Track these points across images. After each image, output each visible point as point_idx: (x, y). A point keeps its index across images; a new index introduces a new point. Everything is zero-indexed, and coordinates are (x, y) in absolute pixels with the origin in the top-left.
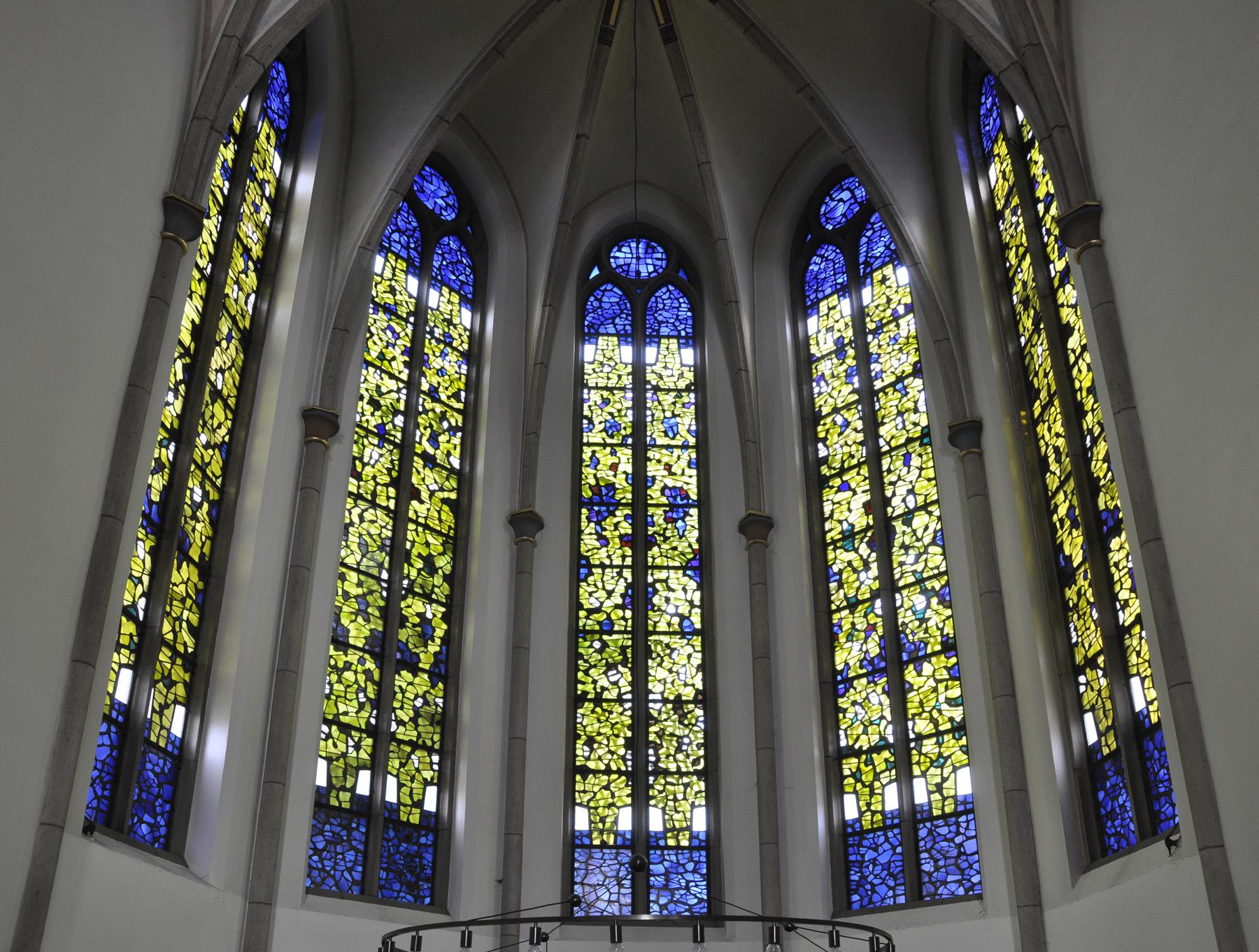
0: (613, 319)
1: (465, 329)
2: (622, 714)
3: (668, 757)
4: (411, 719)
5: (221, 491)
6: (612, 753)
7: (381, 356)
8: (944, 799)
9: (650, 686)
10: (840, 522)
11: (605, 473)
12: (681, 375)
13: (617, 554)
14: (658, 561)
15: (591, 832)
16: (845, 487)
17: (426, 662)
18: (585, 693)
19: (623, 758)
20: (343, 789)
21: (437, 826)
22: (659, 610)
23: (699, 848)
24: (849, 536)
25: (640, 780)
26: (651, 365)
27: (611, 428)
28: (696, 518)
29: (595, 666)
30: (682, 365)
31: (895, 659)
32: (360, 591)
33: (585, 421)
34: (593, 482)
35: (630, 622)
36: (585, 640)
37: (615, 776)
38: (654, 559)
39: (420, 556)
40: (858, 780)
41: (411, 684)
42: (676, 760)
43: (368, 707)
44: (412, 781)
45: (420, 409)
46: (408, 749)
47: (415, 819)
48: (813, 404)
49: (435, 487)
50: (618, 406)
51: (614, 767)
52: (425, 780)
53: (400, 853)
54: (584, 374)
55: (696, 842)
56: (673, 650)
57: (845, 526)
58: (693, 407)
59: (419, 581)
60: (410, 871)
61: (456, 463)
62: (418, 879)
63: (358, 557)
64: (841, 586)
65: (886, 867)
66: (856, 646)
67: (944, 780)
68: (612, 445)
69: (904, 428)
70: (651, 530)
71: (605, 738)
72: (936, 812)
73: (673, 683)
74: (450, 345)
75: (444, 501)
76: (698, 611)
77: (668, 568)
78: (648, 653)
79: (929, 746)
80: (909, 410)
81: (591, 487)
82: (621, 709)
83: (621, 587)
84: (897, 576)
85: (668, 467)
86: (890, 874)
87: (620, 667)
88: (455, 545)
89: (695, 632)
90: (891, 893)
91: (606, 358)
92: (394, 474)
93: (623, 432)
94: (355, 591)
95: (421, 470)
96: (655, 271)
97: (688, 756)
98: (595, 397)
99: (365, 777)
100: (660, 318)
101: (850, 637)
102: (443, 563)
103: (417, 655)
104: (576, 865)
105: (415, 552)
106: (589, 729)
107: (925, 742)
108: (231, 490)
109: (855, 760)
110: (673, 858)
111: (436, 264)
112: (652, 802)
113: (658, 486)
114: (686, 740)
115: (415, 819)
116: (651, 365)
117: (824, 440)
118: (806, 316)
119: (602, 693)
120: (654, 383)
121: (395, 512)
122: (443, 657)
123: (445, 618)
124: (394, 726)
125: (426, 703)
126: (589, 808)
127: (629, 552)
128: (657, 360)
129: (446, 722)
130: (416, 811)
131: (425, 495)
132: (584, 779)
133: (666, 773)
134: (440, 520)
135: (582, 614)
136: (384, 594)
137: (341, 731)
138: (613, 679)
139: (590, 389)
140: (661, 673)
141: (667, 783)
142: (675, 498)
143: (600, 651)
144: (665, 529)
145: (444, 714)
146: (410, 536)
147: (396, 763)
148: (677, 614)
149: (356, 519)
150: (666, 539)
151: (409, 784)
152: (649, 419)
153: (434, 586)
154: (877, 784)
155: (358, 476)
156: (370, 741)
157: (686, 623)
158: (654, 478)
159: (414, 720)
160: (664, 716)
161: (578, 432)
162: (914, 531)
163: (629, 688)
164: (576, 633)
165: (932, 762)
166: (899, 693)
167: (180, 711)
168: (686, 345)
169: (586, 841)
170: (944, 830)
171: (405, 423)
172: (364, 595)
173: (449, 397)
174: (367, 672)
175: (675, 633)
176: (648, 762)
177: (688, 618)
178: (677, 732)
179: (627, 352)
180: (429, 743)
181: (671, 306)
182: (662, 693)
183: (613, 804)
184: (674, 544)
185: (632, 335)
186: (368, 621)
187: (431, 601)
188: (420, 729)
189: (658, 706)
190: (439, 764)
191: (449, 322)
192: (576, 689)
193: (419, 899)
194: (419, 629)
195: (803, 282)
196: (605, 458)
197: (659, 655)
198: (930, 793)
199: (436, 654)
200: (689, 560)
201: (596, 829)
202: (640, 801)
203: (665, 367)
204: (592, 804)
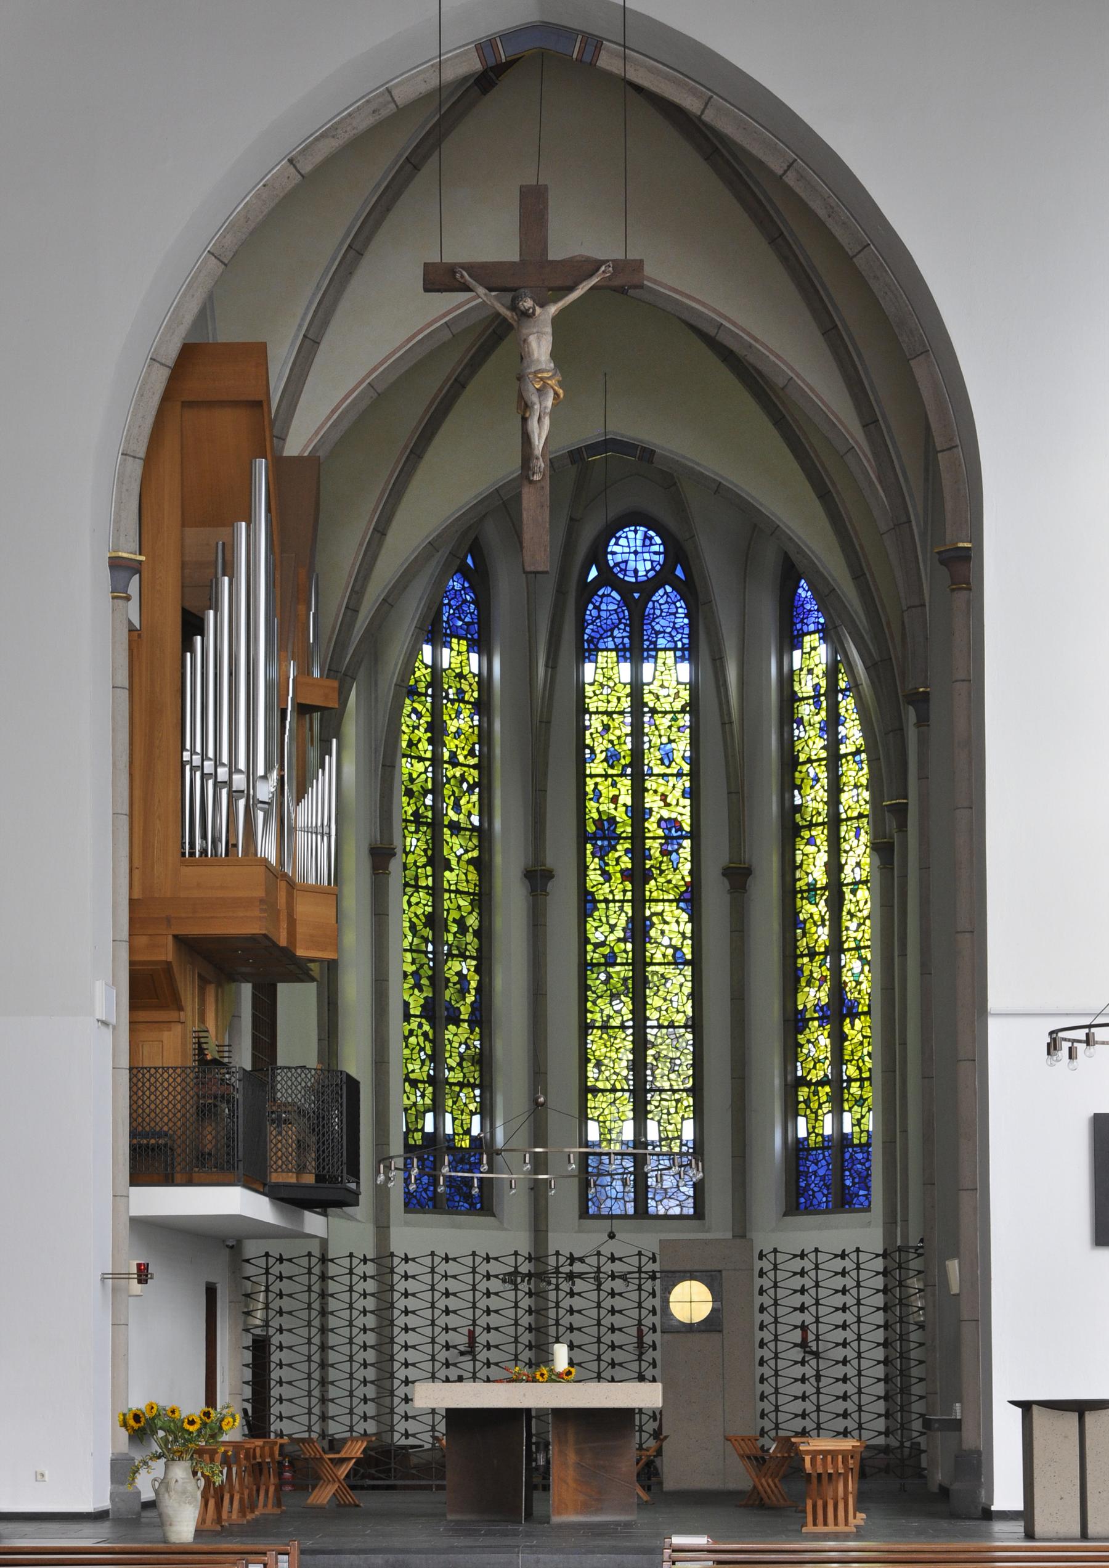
0: (612, 630)
9: (648, 1013)
10: (807, 874)
11: (606, 806)
12: (677, 695)
13: (619, 889)
14: (655, 895)
19: (626, 1079)
22: (656, 942)
25: (640, 1096)
28: (688, 850)
29: (601, 997)
30: (679, 683)
33: (587, 751)
34: (596, 816)
35: (630, 954)
38: (651, 892)
39: (454, 921)
40: (808, 1107)
41: (455, 1035)
42: (669, 1079)
46: (457, 1089)
47: (466, 1144)
50: (618, 733)
51: (618, 1087)
56: (667, 980)
58: (688, 731)
64: (804, 935)
65: (823, 1178)
68: (612, 776)
73: (666, 1010)
76: (689, 942)
77: (663, 901)
78: (645, 982)
81: (594, 821)
82: (623, 1035)
85: (664, 797)
86: (825, 1185)
88: (480, 900)
89: (686, 963)
90: (824, 1199)
93: (623, 762)
95: (449, 840)
96: (653, 568)
97: (679, 1075)
100: (657, 628)
101: (809, 984)
103: (458, 1009)
106: (597, 1053)
109: (807, 1089)
112: (650, 1116)
113: (655, 818)
115: (466, 1144)
119: (608, 1021)
120: (651, 705)
125: (468, 1048)
127: (629, 886)
128: (654, 678)
129: (483, 1060)
132: (595, 1097)
133: (661, 1091)
135: (590, 948)
138: (616, 1008)
139: (591, 714)
141: (662, 1099)
142: (670, 830)
143: (606, 982)
144: (661, 862)
145: (481, 1054)
147: (450, 1102)
148: (671, 946)
152: (646, 746)
154: (820, 1112)
157: (678, 955)
158: (651, 809)
159: (460, 1064)
160: (659, 1041)
161: (581, 762)
163: (630, 1016)
168: (683, 659)
176: (646, 1081)
177: (680, 949)
178: (671, 1055)
180: (472, 1081)
182: (658, 1020)
184: (669, 877)
185: (630, 650)
187: (465, 958)
188: (465, 1070)
189: (655, 1031)
192: (586, 1018)
194: (458, 986)
196: (607, 791)
199: (472, 1004)
200: (682, 893)
202: (640, 1115)
203: (662, 686)
204: (601, 1119)
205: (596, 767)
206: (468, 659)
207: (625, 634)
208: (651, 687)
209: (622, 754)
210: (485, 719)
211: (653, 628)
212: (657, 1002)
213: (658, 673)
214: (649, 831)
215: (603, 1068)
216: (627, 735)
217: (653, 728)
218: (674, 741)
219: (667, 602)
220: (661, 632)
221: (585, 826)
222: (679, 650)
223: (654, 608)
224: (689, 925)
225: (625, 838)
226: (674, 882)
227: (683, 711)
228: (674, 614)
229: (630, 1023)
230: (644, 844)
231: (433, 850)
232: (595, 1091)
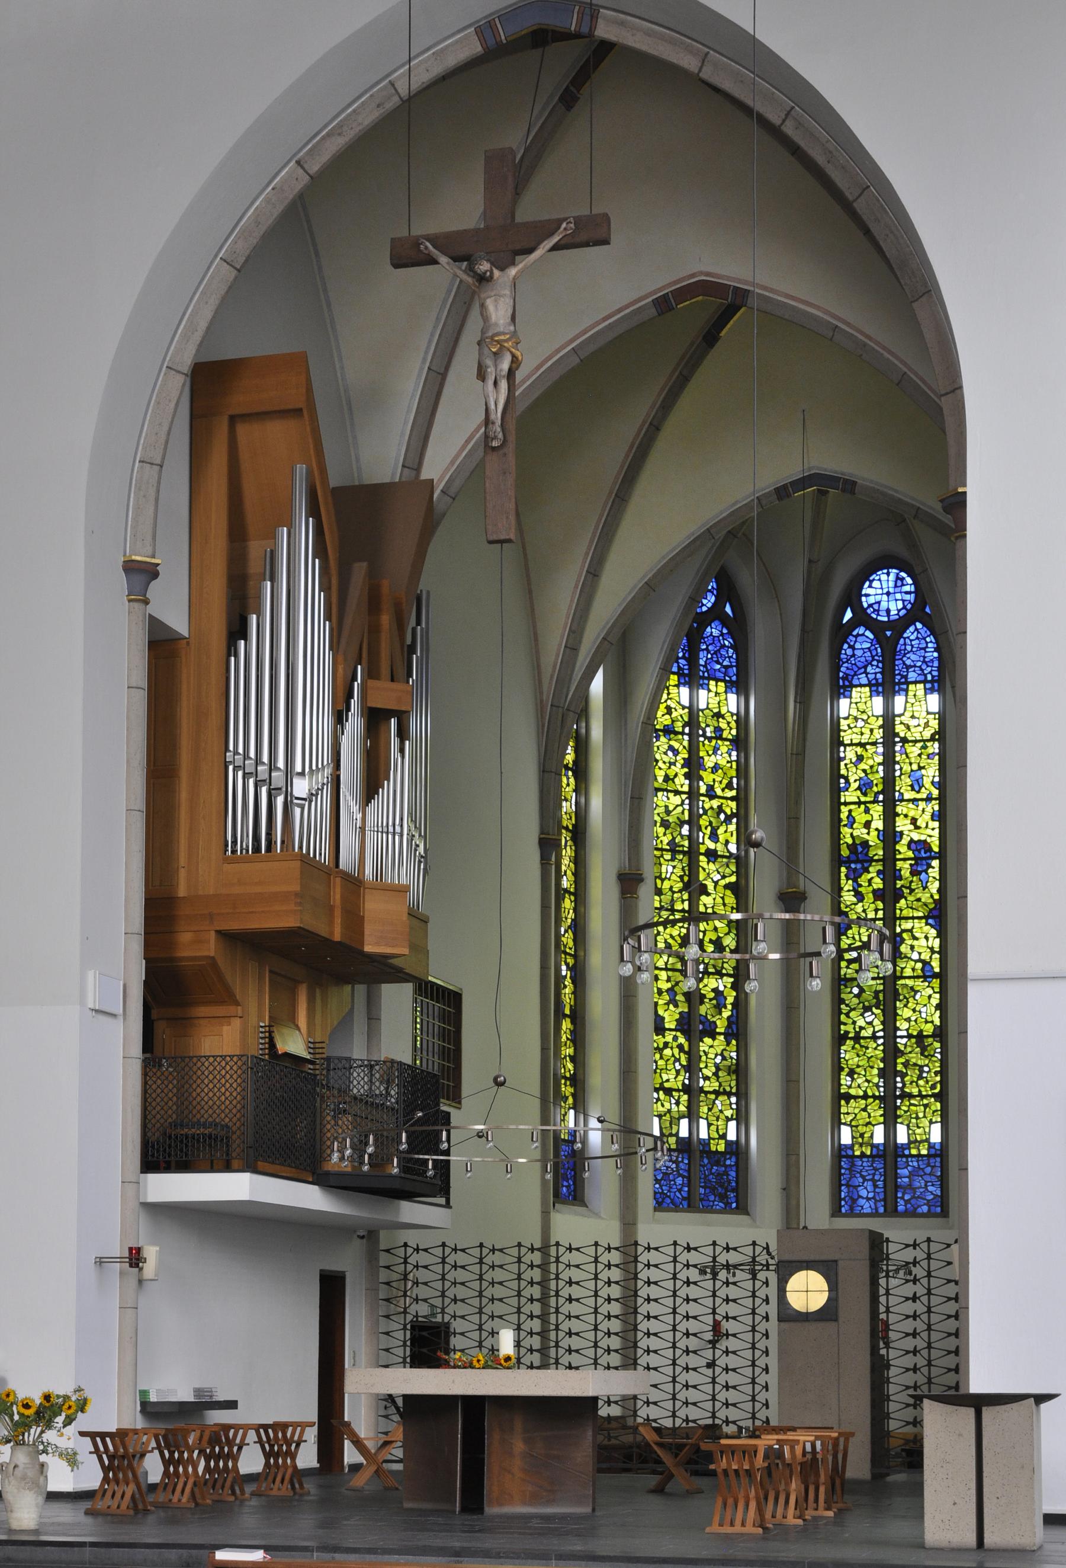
0: (865, 667)
1: (732, 715)
2: (876, 1049)
3: (911, 1083)
4: (714, 1074)
6: (868, 1081)
7: (667, 779)
11: (860, 832)
12: (927, 725)
13: (871, 909)
14: (905, 913)
15: (853, 1145)
17: (721, 1026)
18: (847, 1032)
19: (877, 1086)
20: (671, 1135)
21: (737, 1150)
22: (906, 957)
23: (935, 1156)
26: (899, 716)
27: (865, 786)
28: (937, 869)
29: (854, 1009)
30: (928, 713)
32: (669, 985)
33: (842, 781)
34: (850, 841)
36: (846, 987)
37: (871, 1100)
38: (901, 910)
39: (711, 941)
41: (711, 1046)
42: (918, 1086)
43: (682, 1072)
44: (717, 1120)
45: (701, 811)
46: (713, 1096)
47: (721, 1148)
49: (717, 877)
50: (870, 762)
51: (870, 1093)
52: (727, 1117)
53: (712, 1174)
54: (840, 730)
55: (933, 1151)
56: (916, 992)
58: (937, 757)
60: (721, 1186)
62: (727, 1190)
68: (865, 803)
70: (899, 884)
73: (916, 1021)
76: (937, 956)
77: (913, 918)
78: (896, 996)
81: (848, 846)
82: (875, 1045)
85: (914, 821)
87: (874, 1009)
89: (935, 976)
93: (875, 789)
95: (705, 866)
96: (904, 607)
97: (927, 1082)
98: (850, 754)
99: (684, 1123)
100: (908, 662)
102: (729, 941)
103: (715, 1023)
104: (843, 1171)
106: (850, 1062)
110: (915, 1164)
112: (899, 1120)
113: (905, 840)
115: (721, 1148)
116: (899, 716)
119: (860, 1032)
120: (902, 735)
122: (734, 1019)
125: (724, 1058)
126: (852, 1127)
127: (880, 905)
128: (905, 710)
129: (739, 1070)
130: (722, 1142)
132: (847, 1103)
133: (910, 1096)
134: (724, 905)
135: (843, 964)
138: (869, 1019)
139: (845, 746)
140: (907, 1013)
141: (911, 1105)
142: (920, 852)
143: (858, 996)
144: (912, 882)
145: (737, 1064)
147: (705, 1109)
150: (912, 891)
151: (715, 1123)
152: (897, 773)
156: (686, 1097)
158: (901, 833)
159: (716, 1074)
160: (909, 1049)
161: (836, 791)
163: (881, 1027)
168: (932, 690)
169: (850, 1153)
172: (673, 987)
174: (680, 1047)
175: (918, 977)
176: (896, 1088)
178: (919, 1062)
179: (878, 704)
180: (728, 1089)
182: (907, 1030)
183: (869, 1123)
184: (919, 896)
185: (882, 685)
187: (722, 975)
189: (904, 1041)
190: (737, 1104)
192: (840, 1030)
193: (728, 1204)
194: (714, 1002)
196: (860, 817)
197: (905, 997)
199: (728, 1018)
200: (931, 910)
201: (858, 1143)
202: (890, 1120)
203: (913, 717)
204: (853, 1123)
205: (850, 795)
206: (726, 699)
207: (878, 670)
208: (902, 718)
209: (875, 782)
210: (743, 755)
211: (904, 663)
212: (907, 1013)
213: (908, 705)
214: (900, 853)
215: (856, 1076)
216: (879, 764)
217: (904, 756)
218: (924, 768)
219: (917, 638)
220: (911, 667)
221: (839, 850)
222: (929, 682)
223: (905, 644)
224: (938, 940)
225: (877, 861)
226: (923, 900)
227: (932, 739)
228: (924, 649)
229: (881, 1034)
230: (895, 865)
231: (689, 876)
232: (848, 1097)
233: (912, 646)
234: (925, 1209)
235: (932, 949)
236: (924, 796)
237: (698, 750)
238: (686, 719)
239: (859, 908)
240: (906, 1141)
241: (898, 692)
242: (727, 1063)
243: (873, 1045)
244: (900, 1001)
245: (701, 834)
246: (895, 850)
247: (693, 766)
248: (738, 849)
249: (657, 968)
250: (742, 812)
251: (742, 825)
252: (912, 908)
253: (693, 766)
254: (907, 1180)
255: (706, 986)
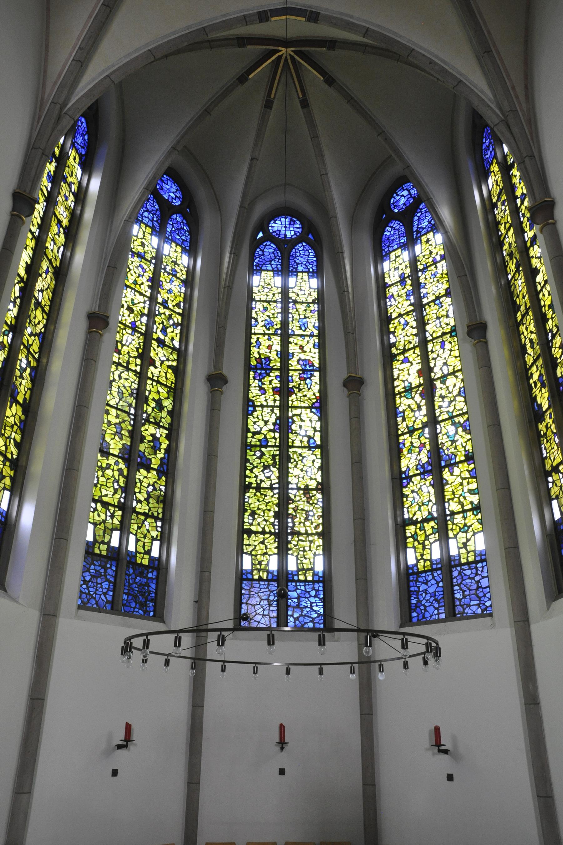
0: (271, 261)
1: (184, 267)
2: (272, 496)
3: (300, 523)
4: (145, 499)
5: (38, 361)
6: (266, 521)
7: (135, 282)
8: (468, 552)
9: (290, 479)
10: (403, 381)
11: (264, 351)
12: (310, 294)
13: (271, 399)
14: (295, 404)
15: (252, 571)
16: (406, 360)
17: (155, 464)
18: (250, 483)
19: (273, 524)
20: (103, 542)
21: (159, 566)
22: (296, 433)
23: (318, 582)
24: (409, 390)
25: (283, 538)
26: (292, 288)
27: (268, 325)
28: (318, 377)
29: (257, 467)
30: (310, 288)
31: (437, 465)
32: (117, 421)
33: (253, 320)
34: (257, 356)
35: (278, 440)
36: (251, 451)
37: (268, 535)
38: (293, 402)
39: (154, 399)
40: (416, 540)
41: (146, 477)
42: (305, 526)
43: (120, 492)
44: (145, 538)
45: (157, 313)
46: (143, 518)
47: (146, 562)
48: (387, 312)
49: (164, 358)
50: (273, 312)
51: (267, 530)
52: (152, 537)
53: (136, 583)
54: (253, 293)
55: (316, 578)
56: (303, 457)
57: (407, 384)
58: (316, 313)
59: (153, 414)
60: (142, 595)
61: (177, 344)
62: (147, 600)
63: (117, 400)
64: (404, 420)
65: (433, 595)
66: (414, 456)
67: (468, 540)
68: (269, 334)
69: (441, 326)
70: (291, 385)
71: (262, 510)
72: (463, 561)
73: (303, 478)
74: (175, 276)
75: (169, 367)
76: (319, 433)
77: (301, 407)
78: (289, 459)
79: (458, 519)
80: (443, 316)
81: (256, 359)
82: (272, 494)
83: (273, 419)
84: (437, 414)
85: (302, 347)
86: (436, 600)
87: (271, 467)
88: (174, 393)
89: (317, 447)
90: (436, 612)
91: (265, 284)
92: (140, 351)
93: (275, 327)
94: (114, 420)
95: (156, 348)
96: (295, 234)
97: (312, 523)
98: (259, 306)
99: (116, 535)
100: (298, 261)
101: (410, 451)
103: (150, 460)
104: (243, 592)
105: (151, 397)
106: (252, 506)
107: (456, 516)
108: (44, 361)
109: (413, 527)
110: (303, 588)
111: (169, 230)
112: (290, 552)
113: (296, 358)
114: (311, 513)
115: (146, 562)
116: (292, 288)
117: (394, 333)
118: (383, 261)
119: (260, 483)
120: (294, 298)
121: (140, 373)
122: (165, 461)
123: (168, 437)
124: (135, 504)
125: (155, 489)
126: (252, 555)
127: (278, 397)
128: (296, 285)
129: (167, 501)
130: (147, 557)
131: (158, 363)
132: (249, 537)
133: (299, 534)
134: (167, 378)
135: (249, 435)
136: (132, 422)
137: (103, 507)
138: (267, 475)
139: (256, 301)
140: (296, 472)
141: (299, 540)
142: (305, 366)
143: (260, 458)
144: (300, 384)
145: (165, 496)
146: (148, 387)
147: (135, 526)
148: (306, 436)
149: (117, 378)
150: (300, 390)
151: (142, 539)
152: (291, 319)
153: (161, 417)
154: (427, 542)
155: (119, 352)
156: (120, 513)
157: (312, 441)
158: (293, 354)
159: (147, 500)
160: (298, 498)
161: (249, 326)
162: (447, 387)
163: (277, 481)
164: (246, 447)
165: (460, 529)
166: (440, 486)
167: (7, 494)
168: (313, 277)
169: (250, 576)
170: (468, 572)
171: (148, 321)
172: (120, 423)
173: (174, 306)
174: (120, 470)
175: (305, 447)
176: (288, 527)
177: (313, 438)
178: (306, 508)
179: (278, 281)
180: (156, 514)
181: (304, 254)
182: (297, 484)
183: (266, 553)
184: (305, 393)
185: (281, 271)
186: (121, 439)
187: (160, 427)
188: (150, 505)
189: (294, 492)
190: (161, 527)
191: (175, 263)
192: (245, 481)
193: (146, 612)
194: (152, 444)
195: (381, 241)
196: (265, 342)
197: (295, 460)
198: (459, 548)
199: (161, 459)
200: (314, 403)
201: (256, 569)
202: (283, 550)
203: (300, 289)
204: (253, 553)
205: (258, 329)
206: (181, 256)
207: (278, 263)
208: (294, 290)
209: (275, 323)
210: (189, 290)
211: (295, 261)
212: (296, 472)
213: (297, 283)
214: (292, 366)
215: (256, 516)
216: (278, 313)
217: (295, 310)
218: (308, 317)
219: (303, 250)
220: (300, 264)
221: (250, 361)
222: (311, 272)
223: (296, 252)
224: (319, 423)
225: (276, 370)
226: (308, 396)
227: (313, 302)
228: (308, 256)
229: (277, 486)
230: (289, 373)
231: (143, 349)
232: (250, 532)
233: (300, 254)
234: (311, 625)
235: (315, 429)
236: (309, 334)
237: (160, 276)
238: (154, 255)
239: (262, 398)
240: (295, 569)
241: (292, 276)
242: (157, 493)
243: (270, 493)
244: (292, 463)
245: (155, 327)
246: (289, 364)
247: (155, 283)
248: (180, 345)
249: (109, 405)
250: (185, 323)
251: (185, 331)
252: (300, 401)
253: (155, 283)
254: (296, 600)
255: (146, 430)
